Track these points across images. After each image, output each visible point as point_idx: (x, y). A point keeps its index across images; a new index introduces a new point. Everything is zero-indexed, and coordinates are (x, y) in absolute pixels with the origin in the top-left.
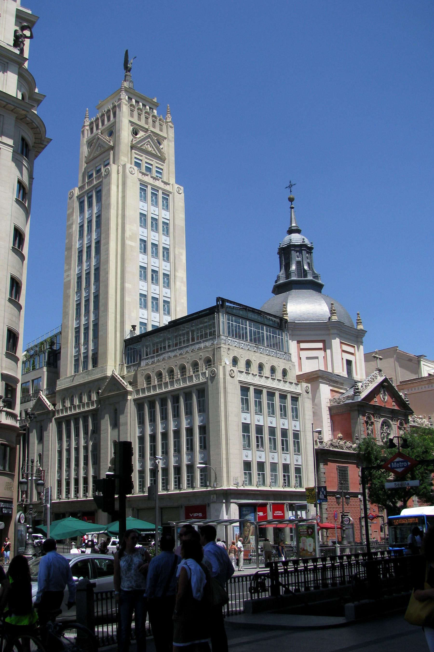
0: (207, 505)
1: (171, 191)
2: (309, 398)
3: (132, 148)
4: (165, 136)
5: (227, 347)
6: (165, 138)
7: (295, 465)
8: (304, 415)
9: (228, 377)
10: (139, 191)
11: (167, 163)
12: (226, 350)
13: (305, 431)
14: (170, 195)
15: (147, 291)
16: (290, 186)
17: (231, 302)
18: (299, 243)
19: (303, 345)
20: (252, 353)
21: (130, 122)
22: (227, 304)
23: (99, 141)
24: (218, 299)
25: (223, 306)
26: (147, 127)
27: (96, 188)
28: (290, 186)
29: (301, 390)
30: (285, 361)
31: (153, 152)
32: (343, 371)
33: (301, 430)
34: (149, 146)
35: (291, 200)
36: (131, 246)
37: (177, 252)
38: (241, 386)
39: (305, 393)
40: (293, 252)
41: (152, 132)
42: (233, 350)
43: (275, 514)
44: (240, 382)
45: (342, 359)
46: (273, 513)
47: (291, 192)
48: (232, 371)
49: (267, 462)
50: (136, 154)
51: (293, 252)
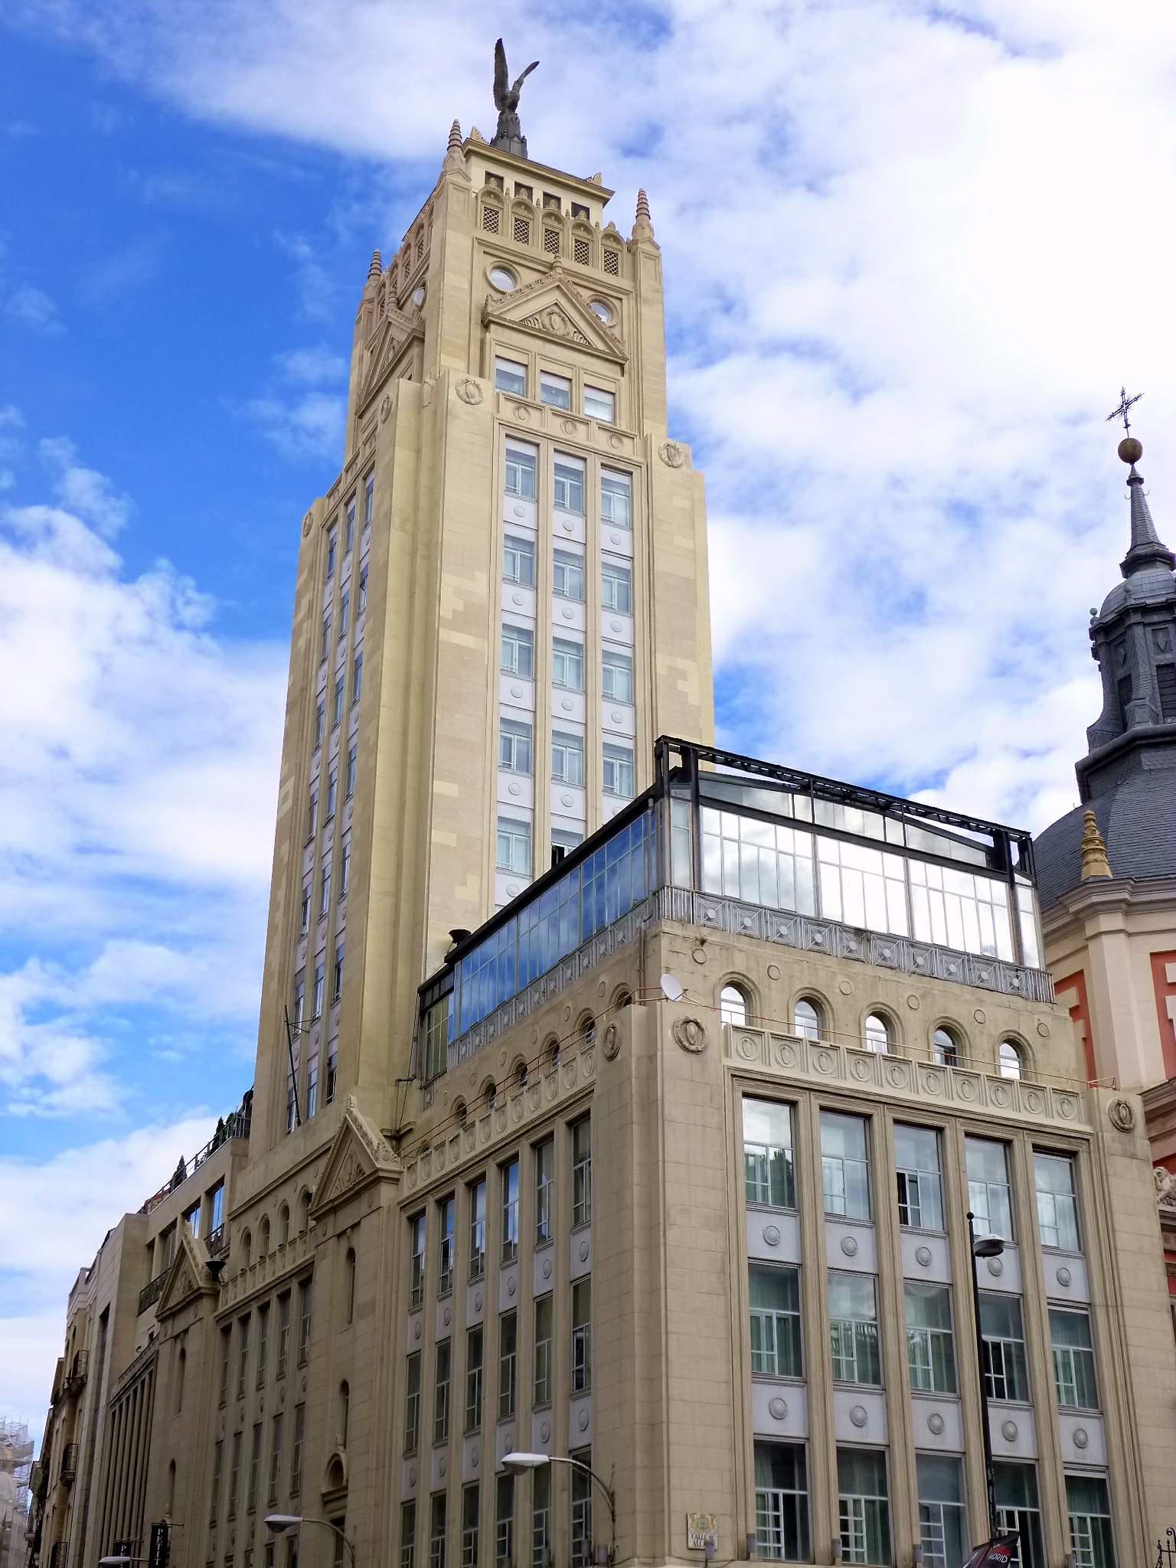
1: (638, 459)
2: (1133, 1157)
3: (486, 325)
4: (625, 283)
5: (692, 932)
6: (627, 293)
7: (1068, 1465)
8: (1111, 1230)
9: (669, 1052)
10: (503, 462)
11: (634, 373)
12: (686, 948)
13: (1116, 1305)
14: (636, 473)
15: (534, 810)
16: (1126, 406)
17: (730, 760)
18: (1163, 599)
21: (481, 242)
22: (704, 766)
23: (393, 331)
24: (662, 746)
25: (686, 775)
26: (550, 257)
28: (1126, 406)
29: (1090, 1121)
30: (1019, 1002)
31: (577, 338)
33: (1098, 1300)
34: (554, 317)
35: (1130, 452)
37: (661, 669)
39: (1110, 1135)
40: (1138, 631)
41: (566, 271)
42: (724, 947)
44: (738, 1076)
47: (1127, 426)
48: (692, 1028)
49: (898, 1449)
50: (500, 344)
51: (1138, 631)
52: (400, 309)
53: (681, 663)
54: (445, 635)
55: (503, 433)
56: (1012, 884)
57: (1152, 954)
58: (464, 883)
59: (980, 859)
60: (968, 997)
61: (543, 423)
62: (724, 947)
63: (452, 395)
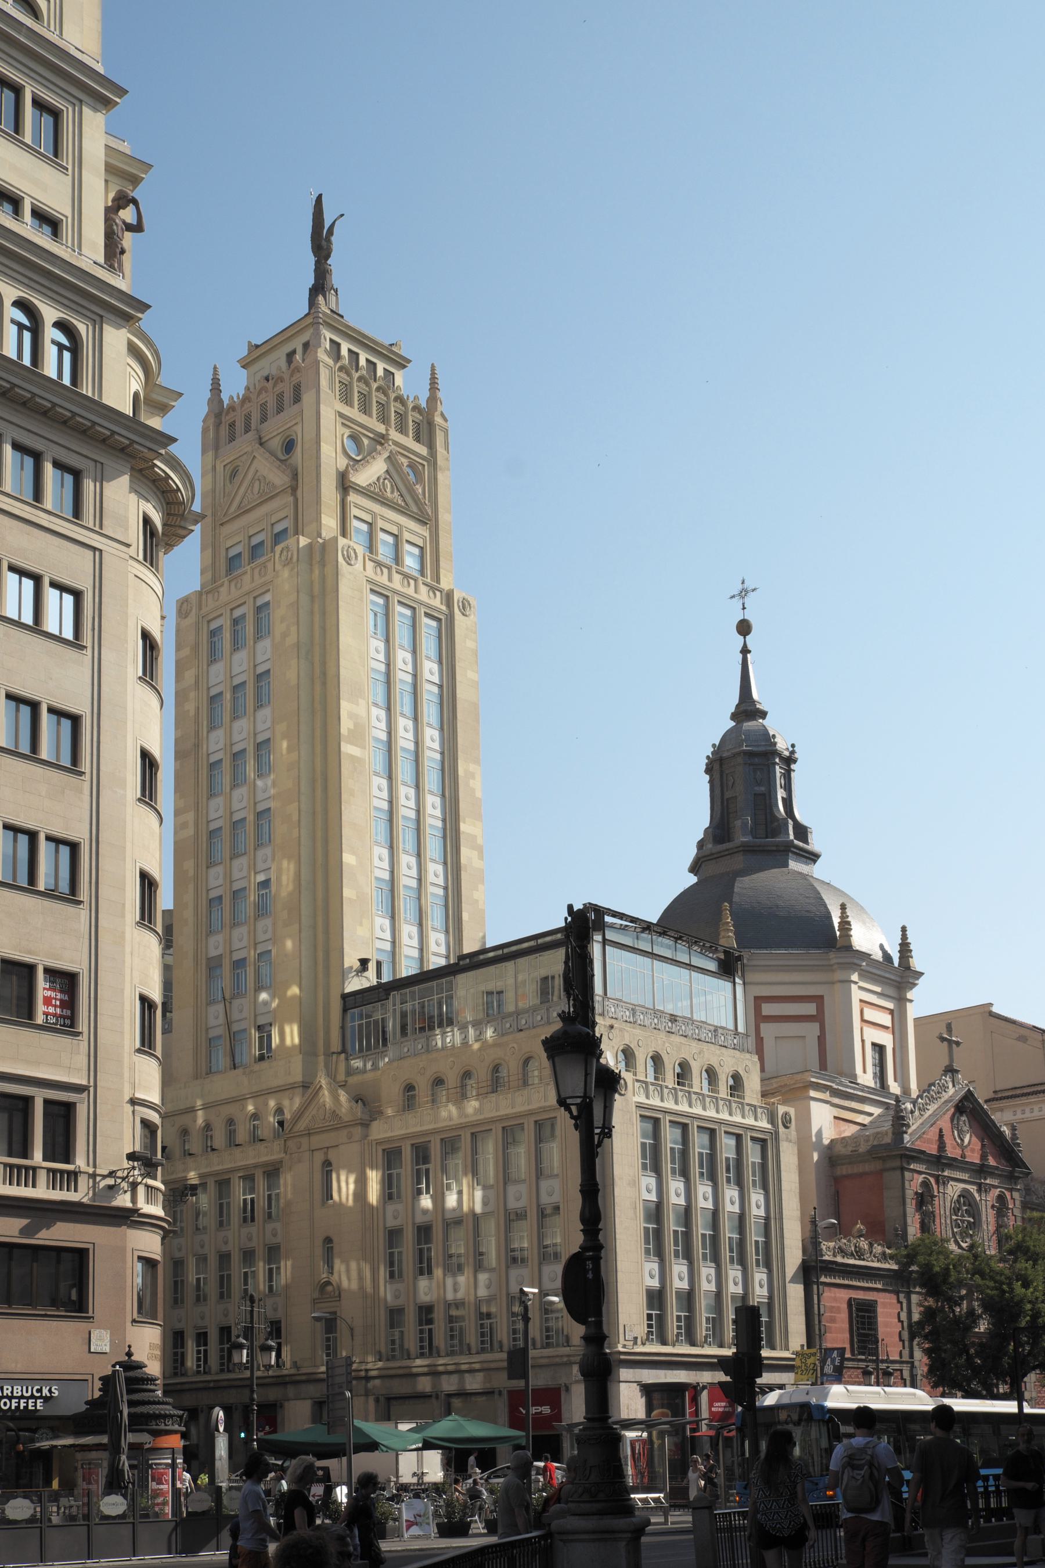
0: (563, 1389)
2: (790, 1141)
19: (768, 1009)
20: (662, 1035)
27: (255, 598)
32: (865, 1072)
36: (353, 758)
38: (641, 1116)
42: (621, 1030)
43: (713, 1409)
44: (639, 1106)
45: (863, 1041)
46: (711, 1405)
50: (357, 506)
52: (261, 444)
53: (472, 767)
54: (347, 748)
55: (369, 587)
56: (734, 983)
57: (755, 998)
58: (361, 924)
59: (712, 966)
60: (718, 1052)
61: (390, 579)
62: (621, 1030)
63: (340, 559)
